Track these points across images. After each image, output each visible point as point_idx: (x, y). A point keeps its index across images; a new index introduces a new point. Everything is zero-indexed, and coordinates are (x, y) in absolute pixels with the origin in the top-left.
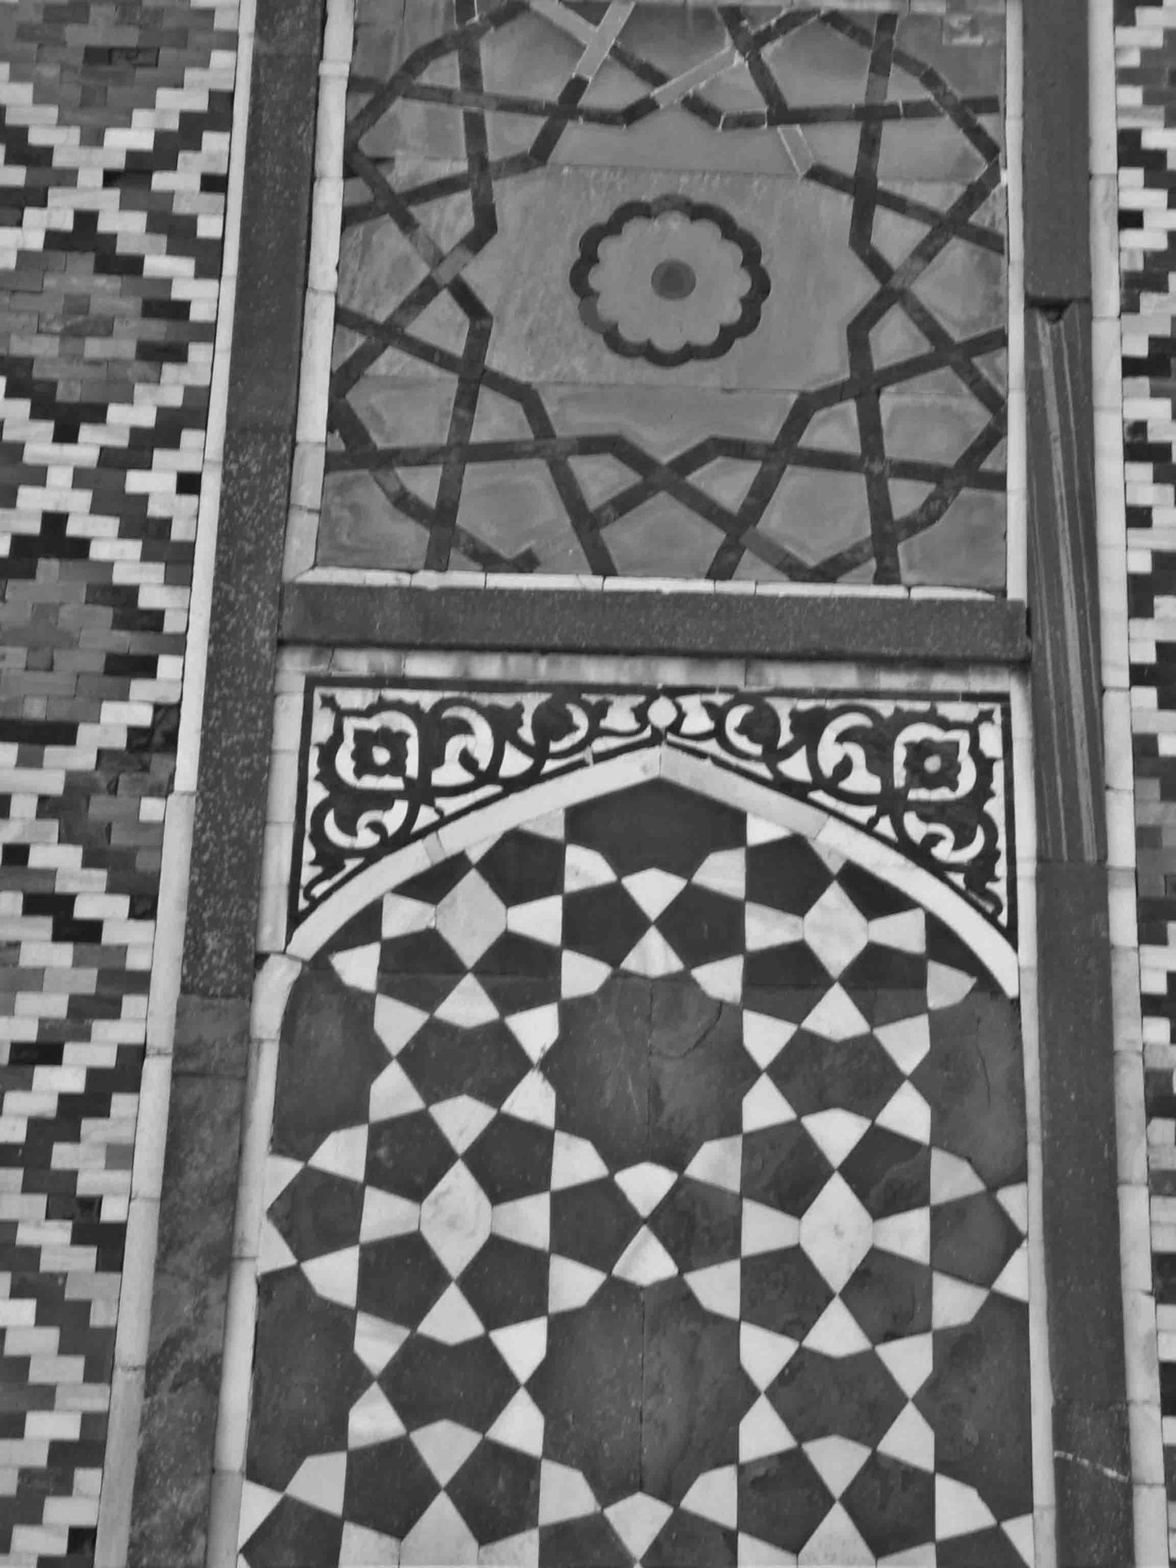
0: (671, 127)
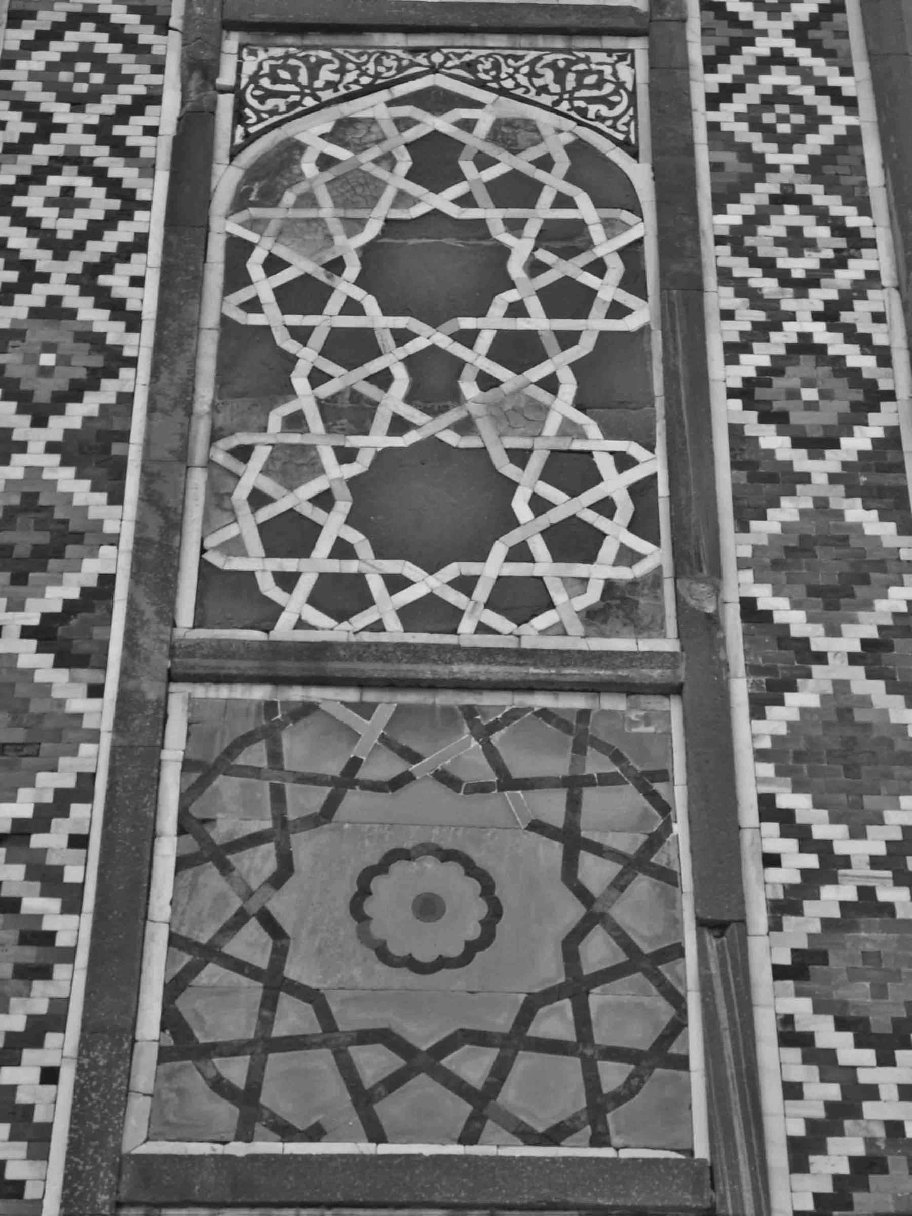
0: (425, 794)
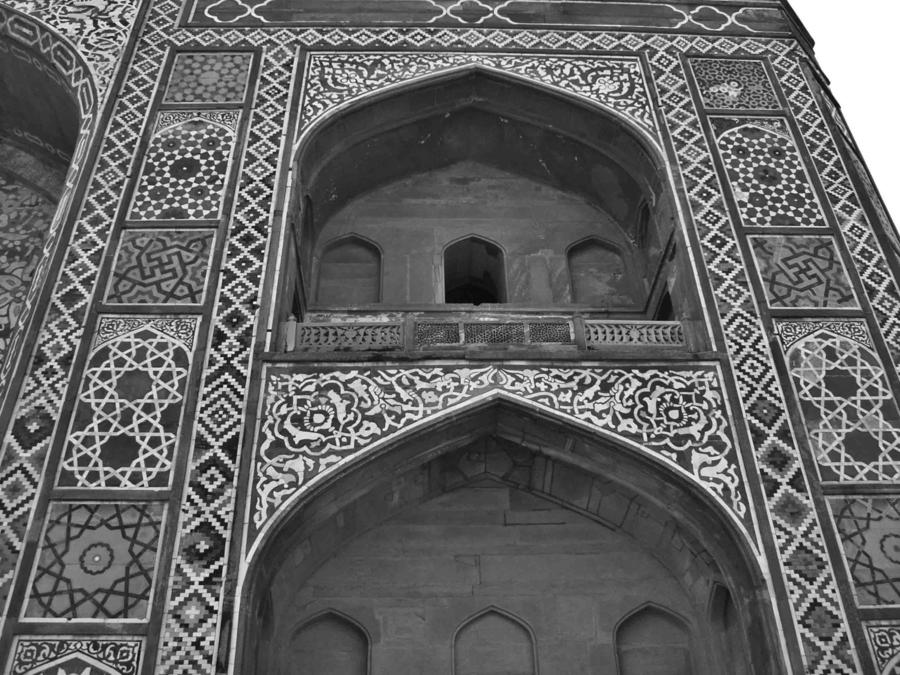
0: (886, 521)
